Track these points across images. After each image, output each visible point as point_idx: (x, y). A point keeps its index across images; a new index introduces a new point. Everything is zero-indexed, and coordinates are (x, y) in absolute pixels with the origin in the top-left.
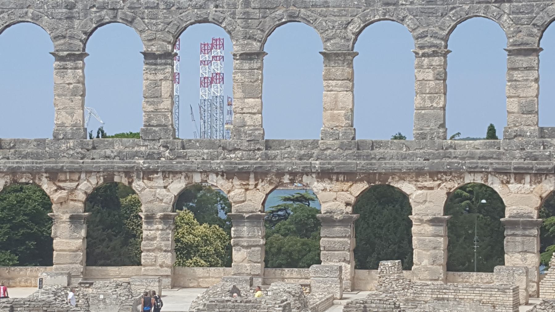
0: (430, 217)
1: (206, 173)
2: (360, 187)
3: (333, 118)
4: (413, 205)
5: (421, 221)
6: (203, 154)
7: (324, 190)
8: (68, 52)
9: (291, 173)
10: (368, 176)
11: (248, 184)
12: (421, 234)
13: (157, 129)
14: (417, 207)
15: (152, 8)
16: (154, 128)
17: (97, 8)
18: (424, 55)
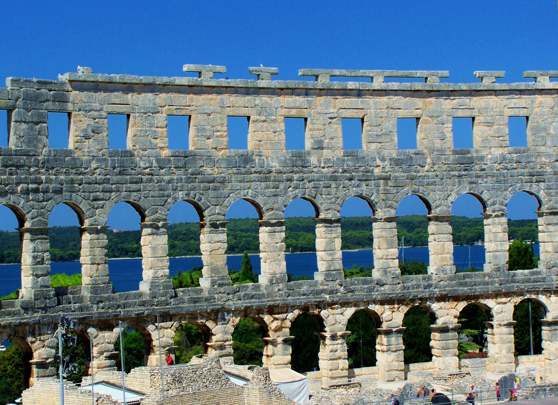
0: (506, 322)
1: (368, 303)
2: (462, 305)
3: (442, 259)
4: (494, 315)
5: (500, 325)
6: (365, 288)
7: (441, 308)
8: (277, 220)
9: (421, 299)
10: (466, 298)
11: (394, 308)
12: (500, 334)
13: (334, 272)
14: (497, 316)
15: (327, 187)
16: (332, 272)
17: (293, 188)
18: (497, 216)
